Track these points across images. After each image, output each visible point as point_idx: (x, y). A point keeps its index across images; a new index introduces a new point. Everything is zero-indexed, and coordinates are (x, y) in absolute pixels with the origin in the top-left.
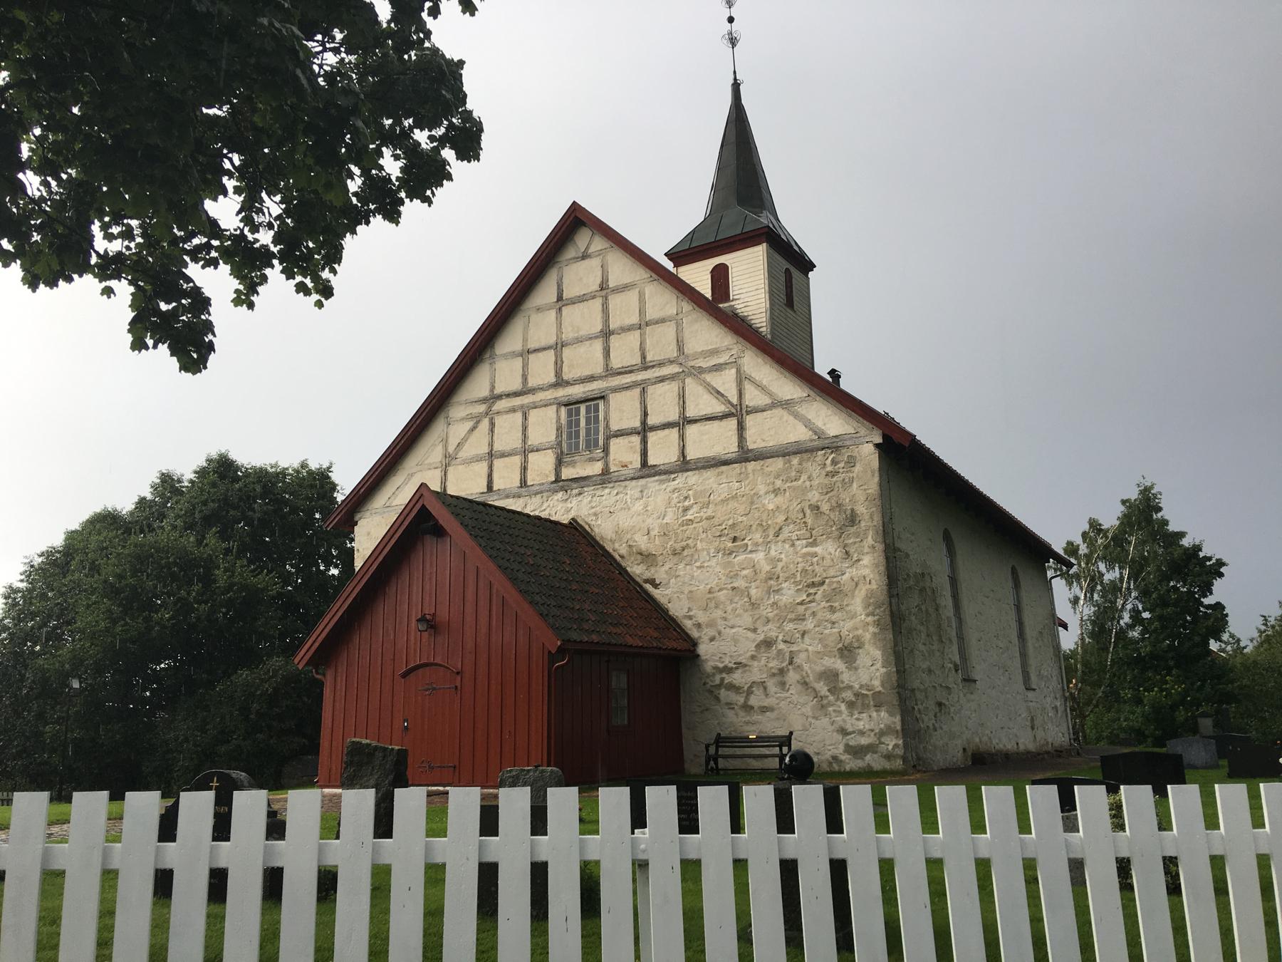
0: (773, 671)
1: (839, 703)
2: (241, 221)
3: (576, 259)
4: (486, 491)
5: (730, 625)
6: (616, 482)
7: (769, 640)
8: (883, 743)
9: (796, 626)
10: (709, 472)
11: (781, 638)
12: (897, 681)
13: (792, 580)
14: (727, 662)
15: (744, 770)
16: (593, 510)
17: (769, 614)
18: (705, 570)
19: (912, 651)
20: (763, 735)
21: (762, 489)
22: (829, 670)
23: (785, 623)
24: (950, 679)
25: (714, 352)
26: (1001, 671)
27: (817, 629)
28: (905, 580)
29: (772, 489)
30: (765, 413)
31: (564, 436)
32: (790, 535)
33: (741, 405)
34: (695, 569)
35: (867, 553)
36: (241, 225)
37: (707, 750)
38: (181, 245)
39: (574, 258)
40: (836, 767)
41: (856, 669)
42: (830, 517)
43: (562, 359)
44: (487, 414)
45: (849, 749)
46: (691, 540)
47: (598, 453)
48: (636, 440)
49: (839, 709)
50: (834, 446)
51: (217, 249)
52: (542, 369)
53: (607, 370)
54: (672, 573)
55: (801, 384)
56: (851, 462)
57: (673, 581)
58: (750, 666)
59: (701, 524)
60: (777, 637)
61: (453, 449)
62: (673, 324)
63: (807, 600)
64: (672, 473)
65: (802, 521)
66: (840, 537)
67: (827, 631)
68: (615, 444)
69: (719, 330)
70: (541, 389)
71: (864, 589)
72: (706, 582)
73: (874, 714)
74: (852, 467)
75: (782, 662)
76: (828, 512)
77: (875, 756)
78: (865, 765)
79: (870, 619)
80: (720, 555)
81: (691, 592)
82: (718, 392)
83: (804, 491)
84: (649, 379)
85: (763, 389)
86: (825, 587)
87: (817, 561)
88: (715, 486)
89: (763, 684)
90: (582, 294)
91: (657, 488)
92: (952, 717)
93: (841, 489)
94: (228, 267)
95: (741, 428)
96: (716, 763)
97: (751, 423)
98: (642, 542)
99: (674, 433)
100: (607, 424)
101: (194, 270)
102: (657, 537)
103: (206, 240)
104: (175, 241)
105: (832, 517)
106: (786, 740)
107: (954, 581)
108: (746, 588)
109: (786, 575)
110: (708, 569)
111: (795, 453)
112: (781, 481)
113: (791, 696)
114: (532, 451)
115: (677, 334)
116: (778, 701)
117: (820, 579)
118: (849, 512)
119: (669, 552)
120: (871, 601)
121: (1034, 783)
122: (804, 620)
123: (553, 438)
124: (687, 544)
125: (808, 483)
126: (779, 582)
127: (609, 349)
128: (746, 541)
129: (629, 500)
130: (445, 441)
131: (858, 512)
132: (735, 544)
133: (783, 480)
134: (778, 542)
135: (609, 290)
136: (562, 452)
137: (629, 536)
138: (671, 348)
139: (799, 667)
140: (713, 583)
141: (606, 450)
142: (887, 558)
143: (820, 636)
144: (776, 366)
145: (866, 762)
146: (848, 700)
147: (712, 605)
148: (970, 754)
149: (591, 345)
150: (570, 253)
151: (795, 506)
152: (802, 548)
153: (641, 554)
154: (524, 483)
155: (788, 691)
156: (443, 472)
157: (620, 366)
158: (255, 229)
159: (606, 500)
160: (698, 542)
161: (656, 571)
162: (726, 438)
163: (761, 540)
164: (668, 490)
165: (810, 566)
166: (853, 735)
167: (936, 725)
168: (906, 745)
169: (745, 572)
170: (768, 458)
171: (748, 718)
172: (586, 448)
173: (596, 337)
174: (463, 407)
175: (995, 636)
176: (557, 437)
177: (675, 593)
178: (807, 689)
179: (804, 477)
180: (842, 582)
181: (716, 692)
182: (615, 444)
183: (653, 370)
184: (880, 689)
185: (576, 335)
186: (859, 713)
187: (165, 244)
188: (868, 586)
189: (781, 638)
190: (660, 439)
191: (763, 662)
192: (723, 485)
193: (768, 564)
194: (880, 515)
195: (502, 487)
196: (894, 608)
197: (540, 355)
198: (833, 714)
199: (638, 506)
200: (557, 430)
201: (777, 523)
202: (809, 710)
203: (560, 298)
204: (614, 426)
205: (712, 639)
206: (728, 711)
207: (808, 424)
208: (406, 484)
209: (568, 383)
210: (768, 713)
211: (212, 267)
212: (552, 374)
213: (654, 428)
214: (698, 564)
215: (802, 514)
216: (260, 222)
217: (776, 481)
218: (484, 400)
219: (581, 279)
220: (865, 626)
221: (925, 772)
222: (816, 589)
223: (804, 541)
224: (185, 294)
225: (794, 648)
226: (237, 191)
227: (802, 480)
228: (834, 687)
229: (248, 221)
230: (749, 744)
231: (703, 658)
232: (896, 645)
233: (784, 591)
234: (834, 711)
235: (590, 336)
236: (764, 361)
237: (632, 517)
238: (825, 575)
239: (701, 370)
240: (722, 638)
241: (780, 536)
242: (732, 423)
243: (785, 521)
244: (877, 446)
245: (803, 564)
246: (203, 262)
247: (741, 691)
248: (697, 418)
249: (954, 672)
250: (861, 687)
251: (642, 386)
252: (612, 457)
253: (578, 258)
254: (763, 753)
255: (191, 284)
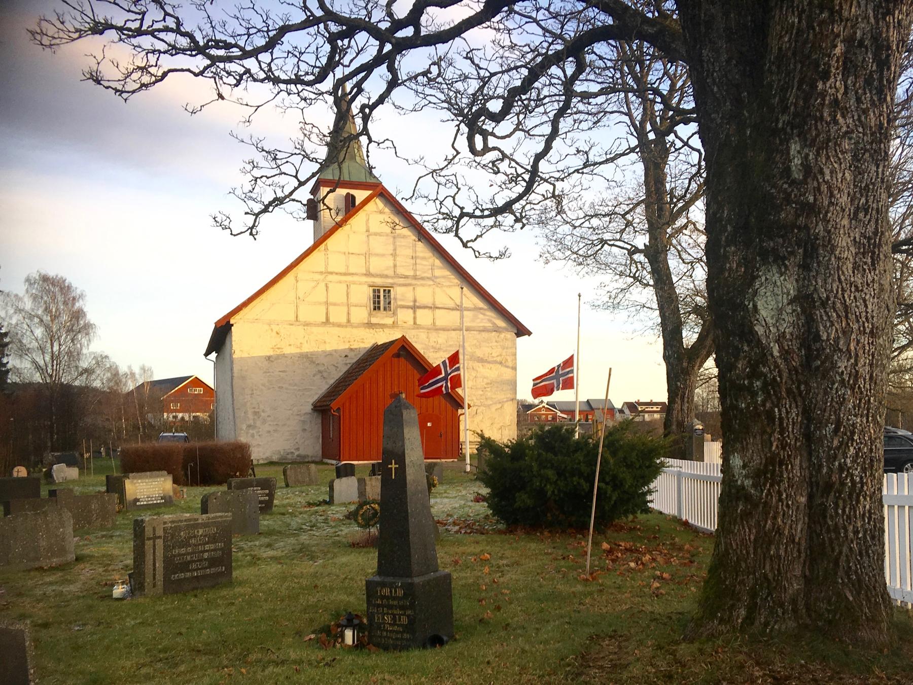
141: (395, 314)
154: (349, 321)
203: (368, 231)
218: (321, 273)
242: (458, 313)
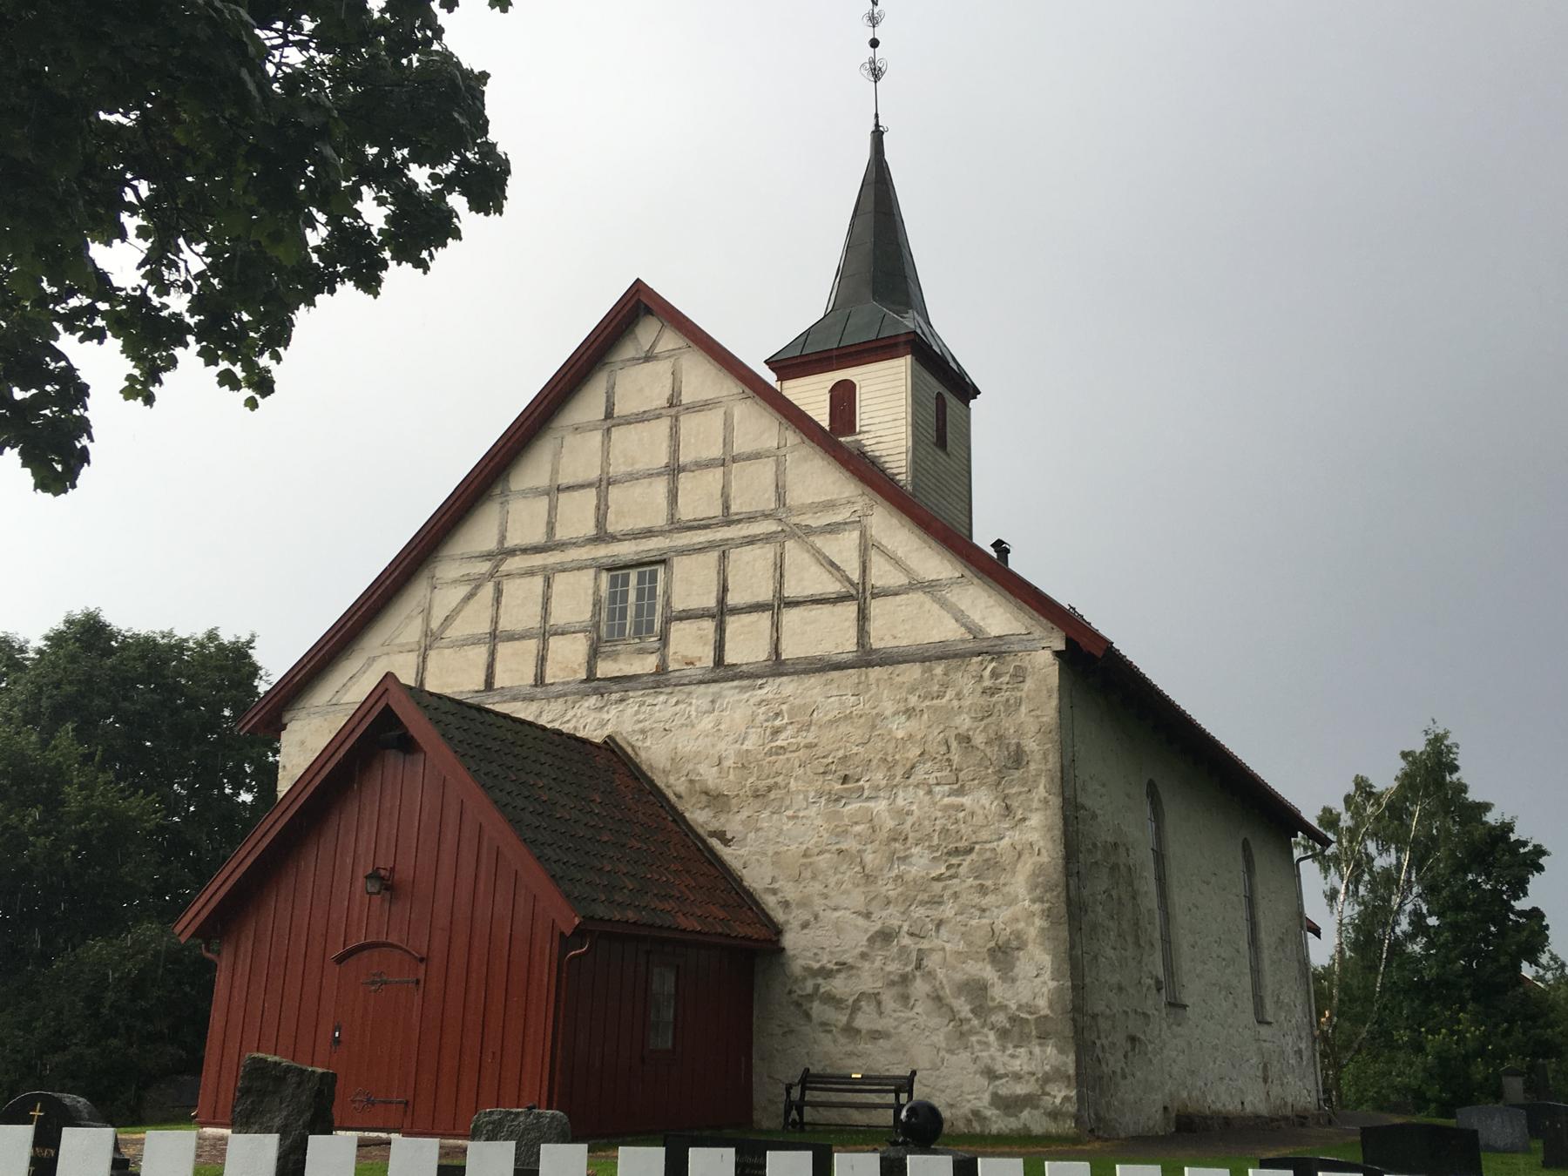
0: (892, 977)
1: (986, 1030)
2: (144, 277)
3: (636, 361)
4: (482, 688)
5: (832, 905)
6: (675, 685)
7: (888, 931)
8: (1049, 1094)
9: (929, 912)
10: (813, 680)
11: (905, 928)
12: (1073, 1001)
13: (927, 844)
14: (826, 961)
15: (842, 1125)
16: (641, 725)
17: (890, 892)
18: (799, 822)
19: (1096, 957)
20: (872, 1074)
21: (888, 707)
22: (974, 980)
23: (913, 908)
24: (1150, 1002)
25: (830, 506)
26: (1223, 993)
27: (959, 918)
28: (1089, 851)
29: (904, 709)
30: (898, 598)
31: (604, 615)
32: (927, 776)
33: (864, 583)
34: (785, 820)
35: (1036, 809)
36: (144, 283)
37: (788, 1093)
38: (51, 306)
39: (634, 359)
40: (978, 1128)
41: (1014, 980)
42: (986, 755)
43: (606, 500)
44: (491, 575)
45: (1000, 1102)
46: (781, 777)
47: (652, 641)
48: (709, 626)
49: (984, 1039)
50: (995, 650)
51: (104, 315)
52: (577, 516)
53: (672, 523)
54: (752, 824)
55: (954, 559)
56: (1020, 675)
57: (752, 835)
58: (858, 969)
59: (797, 754)
60: (900, 927)
61: (439, 624)
62: (771, 462)
63: (948, 874)
64: (759, 677)
65: (945, 757)
66: (999, 784)
67: (974, 922)
68: (678, 631)
69: (837, 475)
70: (574, 544)
71: (1030, 861)
72: (801, 840)
73: (1037, 1050)
74: (1023, 682)
75: (906, 965)
76: (982, 747)
77: (1035, 1112)
78: (1020, 1126)
79: (1037, 907)
80: (823, 800)
81: (777, 853)
82: (832, 564)
83: (951, 713)
84: (733, 539)
85: (897, 563)
86: (974, 856)
87: (964, 818)
88: (820, 699)
89: (875, 997)
90: (642, 410)
91: (737, 697)
92: (1151, 1061)
93: (1002, 715)
94: (119, 343)
95: (863, 617)
96: (801, 1114)
97: (877, 610)
98: (709, 775)
99: (764, 619)
100: (668, 600)
101: (67, 343)
102: (731, 770)
103: (89, 301)
104: (43, 300)
105: (989, 754)
106: (906, 1084)
107: (1160, 857)
108: (859, 851)
109: (918, 835)
110: (804, 821)
111: (939, 658)
112: (916, 698)
113: (917, 1016)
114: (555, 634)
115: (777, 476)
116: (896, 1023)
117: (966, 844)
118: (1012, 748)
119: (748, 793)
120: (1040, 880)
121: (1265, 1164)
122: (940, 903)
123: (587, 616)
124: (776, 783)
125: (955, 703)
126: (908, 845)
127: (677, 493)
128: (861, 783)
129: (694, 714)
130: (427, 613)
131: (1026, 749)
132: (845, 786)
133: (919, 696)
134: (909, 785)
135: (681, 408)
136: (599, 638)
137: (690, 766)
138: (766, 496)
139: (930, 975)
140: (811, 842)
141: (664, 639)
142: (1065, 819)
143: (963, 929)
144: (917, 531)
145: (1022, 1121)
146: (999, 1026)
147: (807, 874)
148: (1174, 1115)
149: (650, 484)
150: (628, 351)
151: (935, 735)
152: (943, 797)
153: (706, 793)
154: (540, 680)
155: (912, 1009)
156: (421, 657)
157: (691, 517)
158: (163, 289)
159: (660, 711)
160: (792, 780)
161: (728, 820)
162: (840, 630)
163: (885, 782)
164: (752, 701)
165: (953, 824)
166: (1004, 1080)
167: (1126, 1070)
168: (1081, 1098)
169: (858, 828)
170: (900, 663)
171: (850, 1048)
172: (635, 633)
173: (659, 474)
174: (458, 563)
175: (1216, 942)
176: (593, 615)
177: (754, 855)
178: (940, 1008)
179: (950, 694)
180: (998, 850)
181: (806, 1006)
182: (678, 631)
183: (739, 526)
184: (1046, 1012)
185: (629, 469)
186: (1016, 1047)
187: (28, 304)
188: (1036, 859)
189: (905, 928)
190: (743, 626)
191: (878, 964)
192: (833, 699)
193: (892, 819)
194: (1057, 755)
195: (507, 684)
196: (1073, 893)
197: (576, 494)
198: (977, 1047)
199: (707, 723)
200: (594, 606)
201: (908, 759)
202: (942, 1038)
203: (609, 415)
204: (678, 605)
205: (805, 925)
206: (822, 1035)
207: (959, 617)
208: (364, 672)
209: (614, 538)
210: (881, 1041)
211: (95, 341)
212: (592, 523)
213: (736, 611)
214: (790, 813)
215: (945, 748)
216: (172, 280)
217: (910, 697)
218: (488, 556)
219: (641, 390)
220: (1029, 917)
221: (1106, 1140)
222: (961, 858)
223: (947, 788)
224: (52, 377)
225: (925, 945)
226: (142, 233)
227: (947, 697)
228: (981, 1006)
229: (154, 277)
230: (850, 1087)
231: (790, 952)
232: (1072, 947)
233: (913, 860)
234: (979, 1042)
235: (650, 472)
236: (900, 523)
237: (697, 739)
238: (974, 840)
239: (809, 531)
240: (819, 925)
241: (912, 777)
242: (851, 609)
243: (920, 756)
244: (1057, 654)
245: (943, 821)
246: (82, 333)
247: (843, 1006)
248: (800, 599)
249: (1155, 991)
250: (1020, 1007)
251: (722, 548)
252: (672, 649)
253: (639, 359)
254: (871, 1101)
255: (63, 364)
